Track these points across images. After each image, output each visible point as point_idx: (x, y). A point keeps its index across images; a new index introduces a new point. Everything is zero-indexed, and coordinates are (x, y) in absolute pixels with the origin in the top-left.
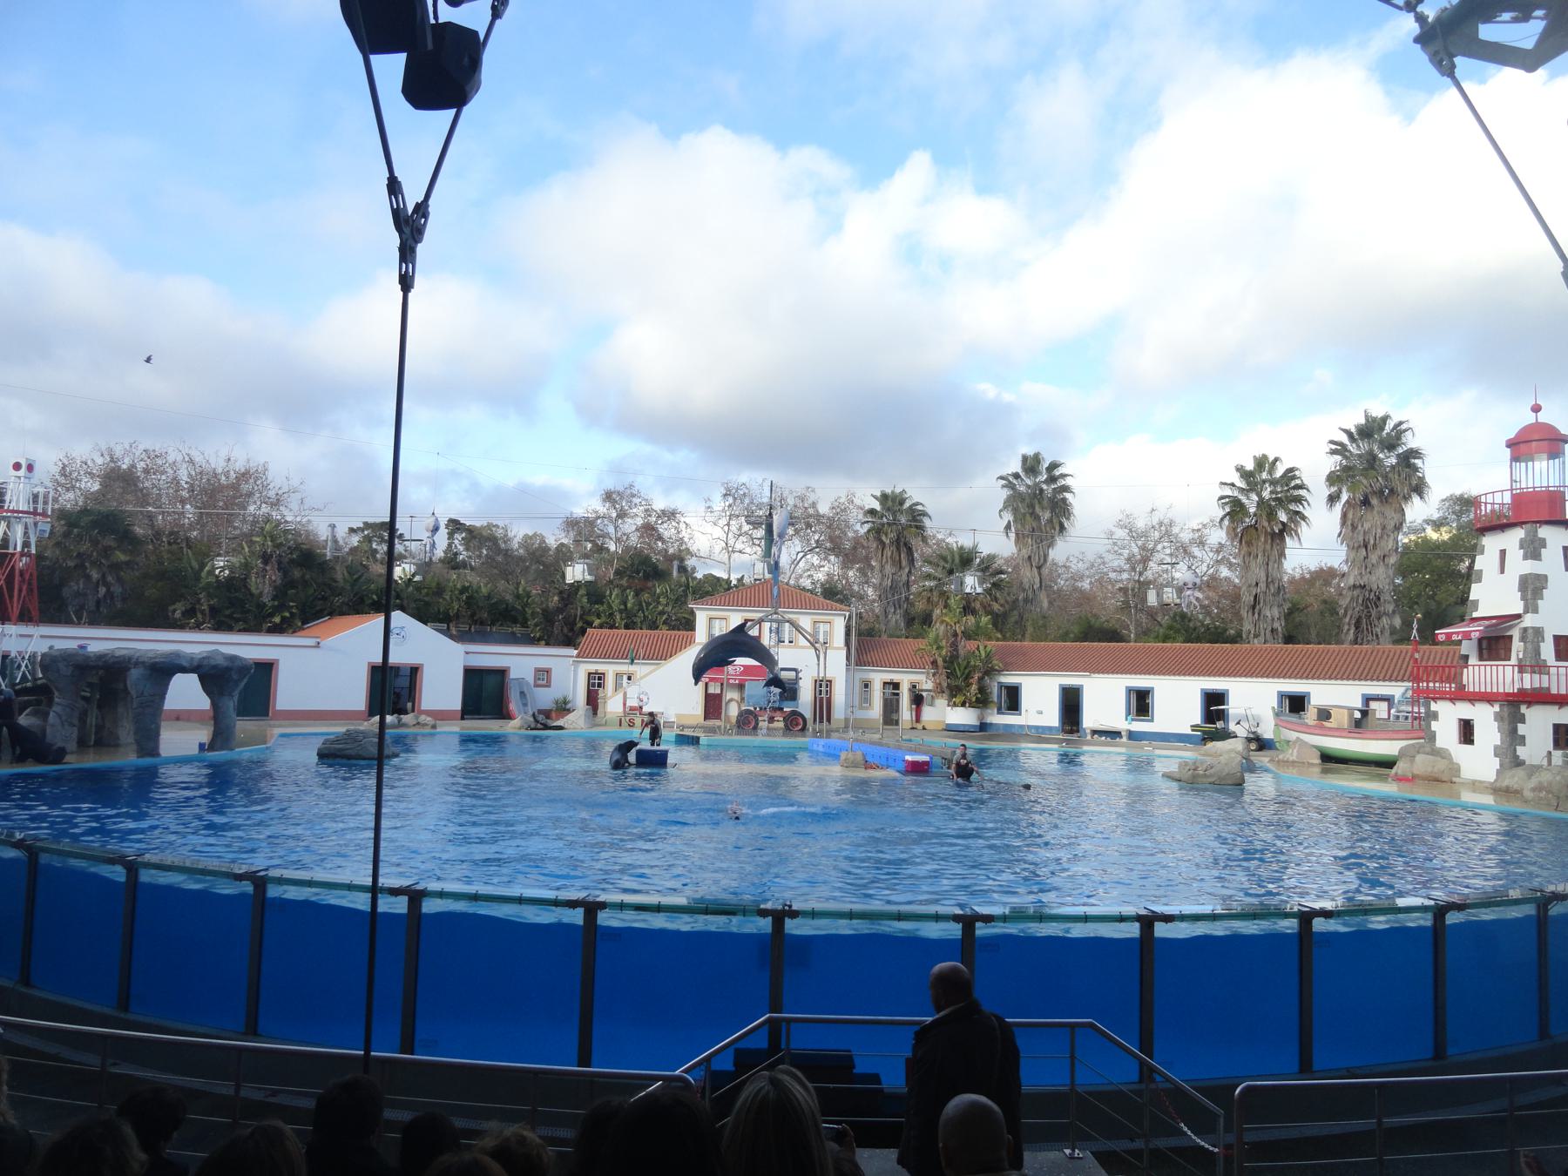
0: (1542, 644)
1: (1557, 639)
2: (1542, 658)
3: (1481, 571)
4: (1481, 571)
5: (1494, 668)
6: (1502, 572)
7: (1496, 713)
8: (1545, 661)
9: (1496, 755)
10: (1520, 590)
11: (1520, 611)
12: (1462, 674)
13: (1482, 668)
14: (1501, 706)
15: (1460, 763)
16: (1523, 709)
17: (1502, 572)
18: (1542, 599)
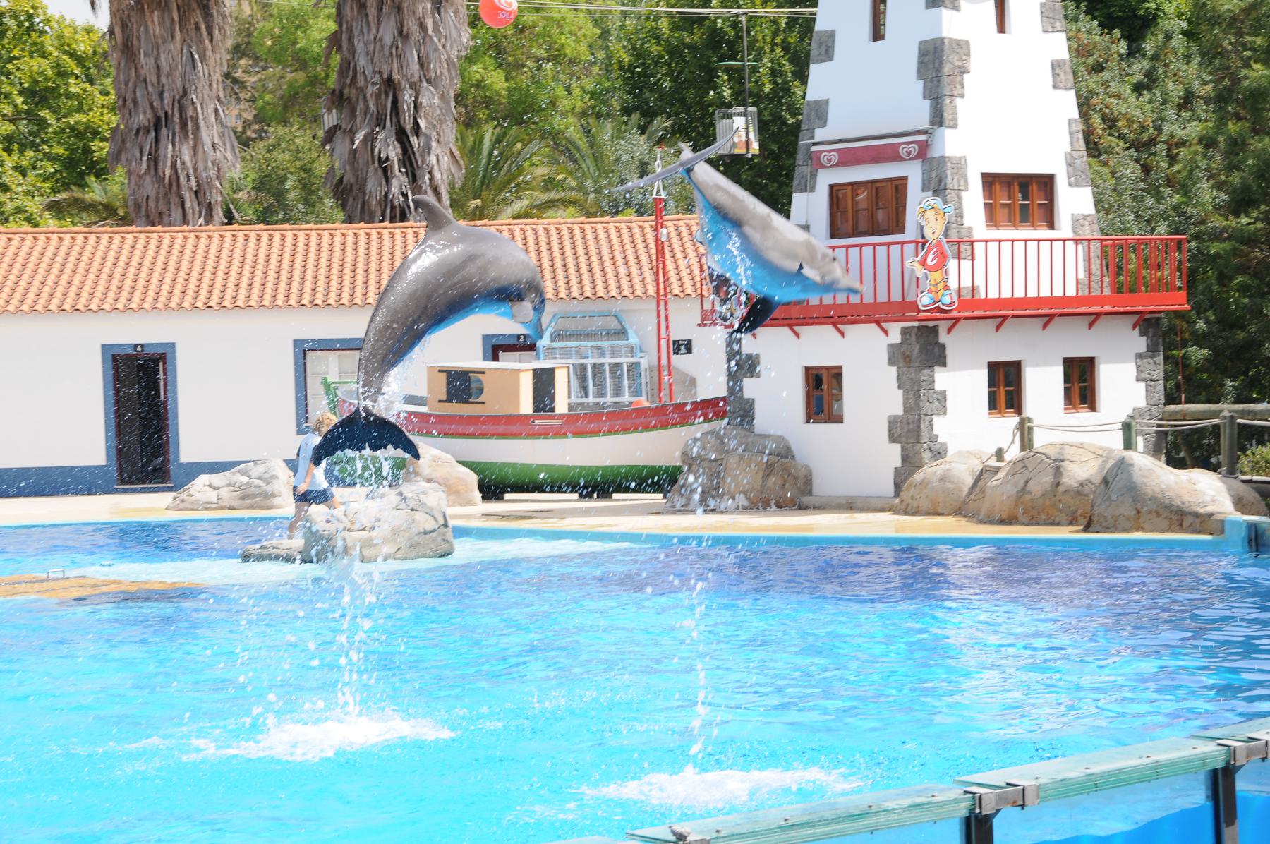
0: (964, 194)
1: (991, 181)
3: (831, 34)
4: (831, 34)
5: (882, 251)
6: (878, 34)
7: (891, 346)
8: (970, 229)
9: (893, 438)
10: (921, 74)
11: (924, 124)
14: (905, 332)
15: (812, 466)
16: (943, 338)
17: (878, 35)
18: (962, 96)
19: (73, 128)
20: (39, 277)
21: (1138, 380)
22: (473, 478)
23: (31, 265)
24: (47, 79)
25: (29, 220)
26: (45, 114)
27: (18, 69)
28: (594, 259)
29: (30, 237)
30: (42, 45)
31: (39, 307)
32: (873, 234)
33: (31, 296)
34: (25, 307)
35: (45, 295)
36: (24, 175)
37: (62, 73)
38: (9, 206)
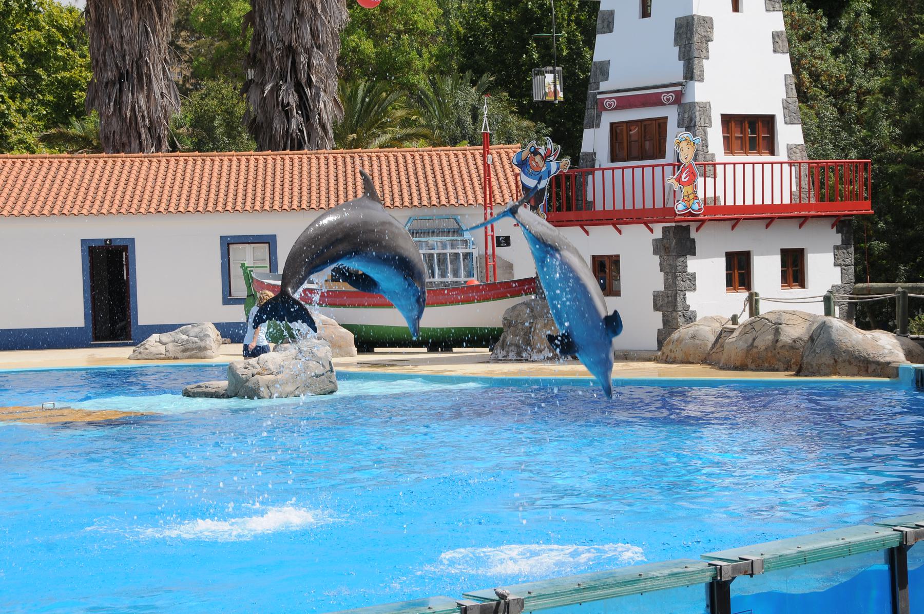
0: (708, 129)
1: (727, 120)
2: (710, 152)
3: (611, 13)
4: (611, 13)
5: (648, 171)
7: (655, 241)
8: (713, 155)
9: (656, 308)
10: (677, 42)
11: (680, 78)
12: (584, 185)
13: (618, 173)
14: (665, 230)
16: (693, 234)
18: (707, 58)
19: (59, 82)
20: (35, 190)
21: (835, 265)
22: (351, 336)
23: (29, 182)
24: (41, 46)
25: (28, 148)
26: (40, 71)
27: (20, 39)
28: (439, 177)
29: (29, 161)
30: (38, 21)
31: (35, 212)
32: (642, 159)
33: (30, 203)
34: (26, 212)
35: (40, 203)
36: (24, 116)
37: (52, 42)
38: (14, 139)
